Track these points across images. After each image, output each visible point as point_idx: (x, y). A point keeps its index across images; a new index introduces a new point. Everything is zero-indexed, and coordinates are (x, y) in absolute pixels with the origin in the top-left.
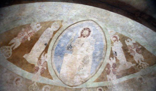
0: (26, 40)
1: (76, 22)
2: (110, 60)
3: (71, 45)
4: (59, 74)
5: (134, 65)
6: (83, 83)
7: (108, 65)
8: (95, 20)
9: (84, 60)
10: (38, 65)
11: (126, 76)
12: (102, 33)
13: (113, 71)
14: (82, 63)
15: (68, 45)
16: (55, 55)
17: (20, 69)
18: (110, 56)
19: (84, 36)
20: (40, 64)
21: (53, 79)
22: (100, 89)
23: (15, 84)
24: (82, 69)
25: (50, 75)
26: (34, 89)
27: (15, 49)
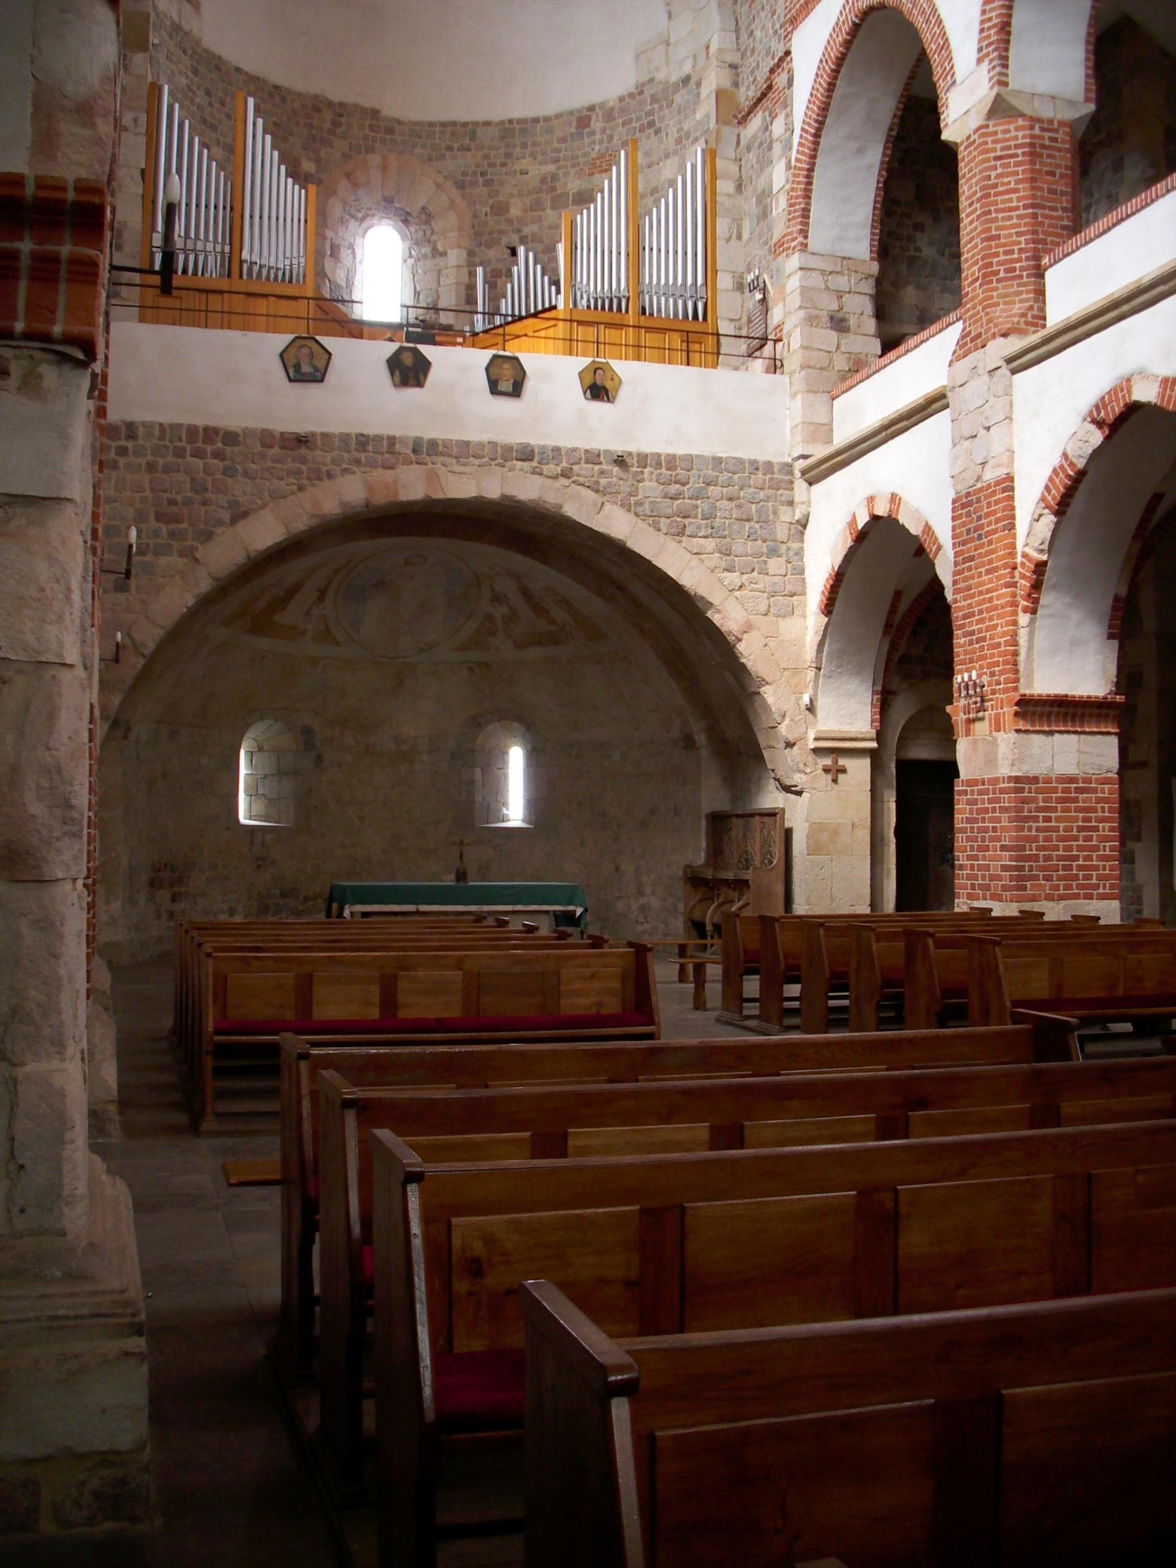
5: (554, 628)
7: (489, 617)
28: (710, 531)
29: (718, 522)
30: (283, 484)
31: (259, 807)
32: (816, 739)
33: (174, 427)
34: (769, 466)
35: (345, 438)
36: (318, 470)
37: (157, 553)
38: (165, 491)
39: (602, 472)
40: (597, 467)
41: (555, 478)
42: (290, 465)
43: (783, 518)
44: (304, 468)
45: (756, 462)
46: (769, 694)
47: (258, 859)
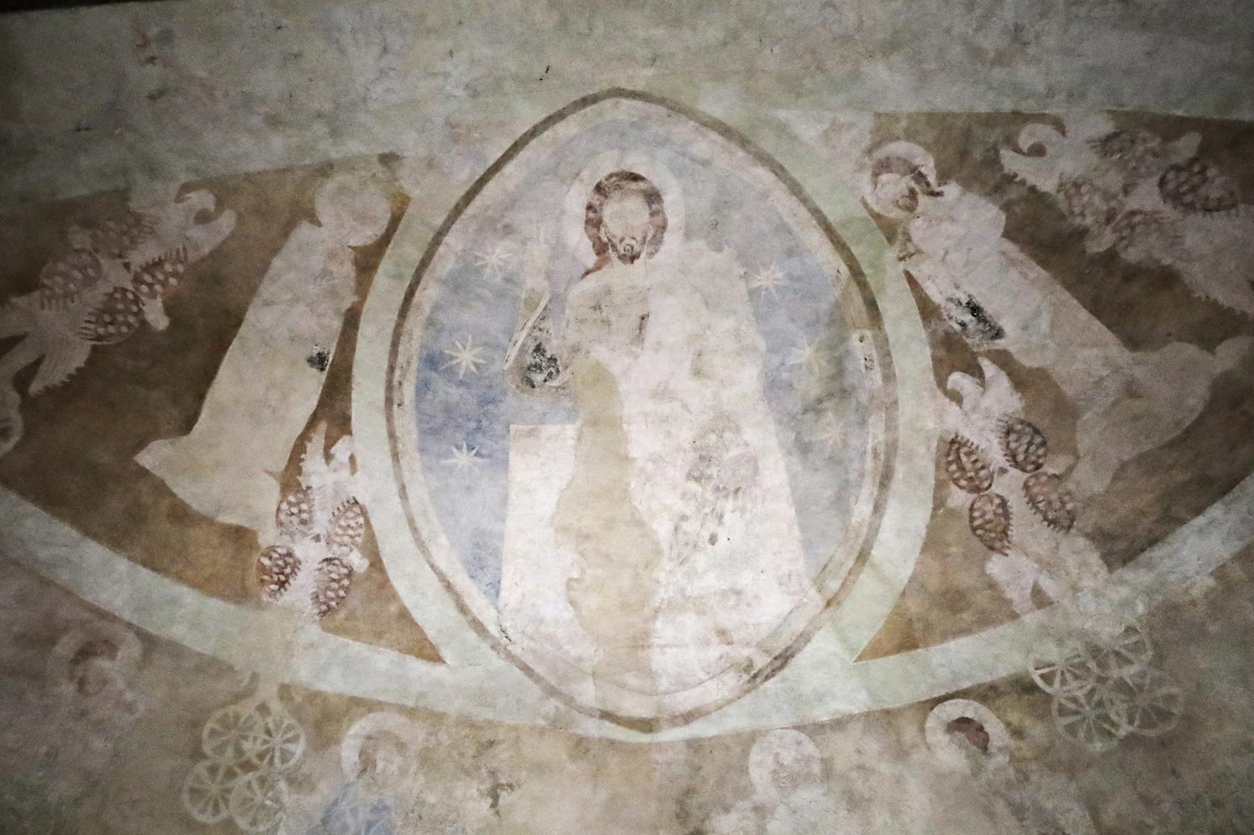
0: (129, 326)
1: (507, 144)
2: (956, 397)
3: (539, 349)
4: (493, 612)
6: (755, 677)
8: (641, 78)
9: (705, 459)
10: (292, 535)
11: (1216, 511)
12: (763, 174)
13: (1033, 501)
14: (693, 486)
15: (513, 352)
16: (422, 450)
17: (122, 564)
18: (937, 362)
19: (621, 248)
20: (303, 522)
21: (445, 653)
22: (961, 724)
23: (67, 689)
24: (713, 540)
25: (413, 623)
26: (259, 747)
27: (48, 391)
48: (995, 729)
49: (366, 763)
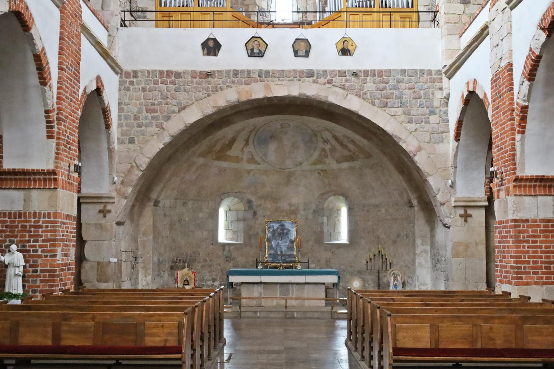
5: (351, 153)
7: (324, 150)
22: (319, 172)
28: (400, 104)
29: (404, 100)
30: (201, 93)
31: (230, 235)
32: (455, 201)
33: (154, 71)
34: (430, 72)
35: (228, 72)
36: (216, 87)
37: (147, 126)
38: (150, 99)
39: (347, 80)
40: (344, 78)
41: (325, 84)
42: (204, 85)
43: (437, 96)
44: (210, 86)
45: (423, 70)
46: (431, 181)
47: (226, 257)
48: (322, 173)
49: (254, 175)
